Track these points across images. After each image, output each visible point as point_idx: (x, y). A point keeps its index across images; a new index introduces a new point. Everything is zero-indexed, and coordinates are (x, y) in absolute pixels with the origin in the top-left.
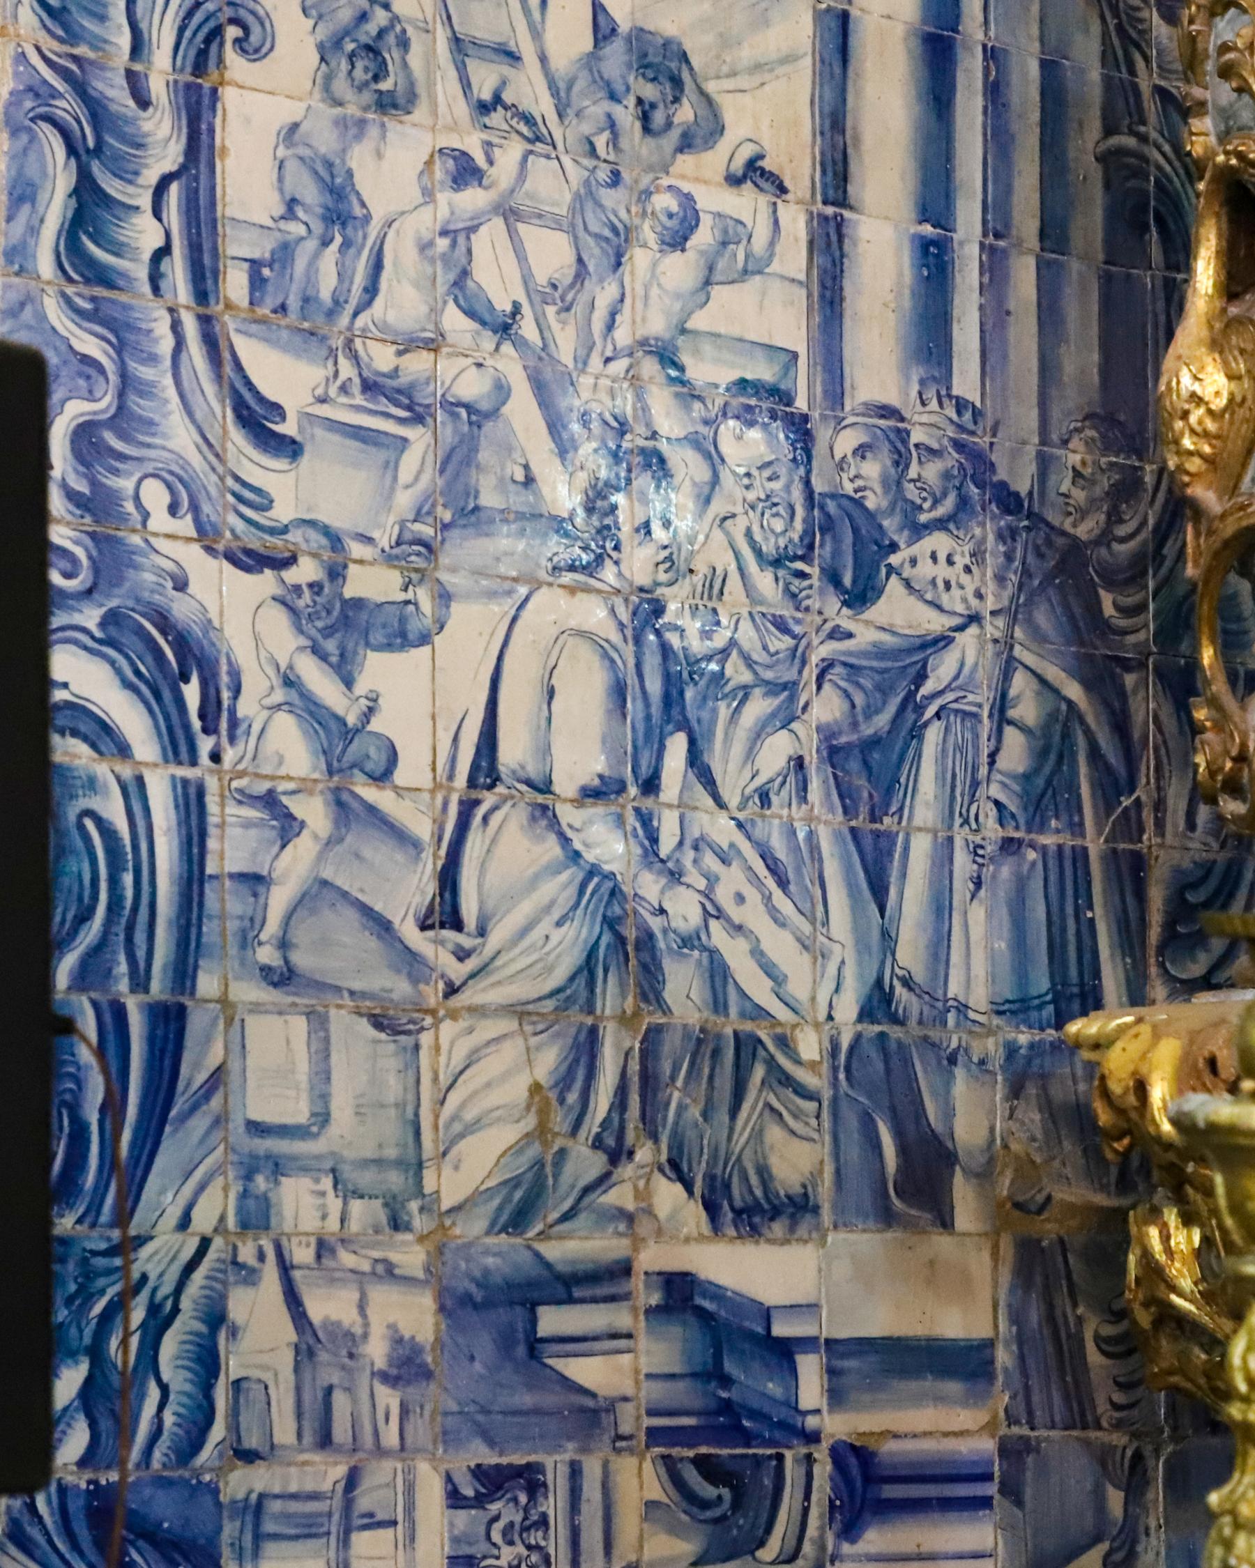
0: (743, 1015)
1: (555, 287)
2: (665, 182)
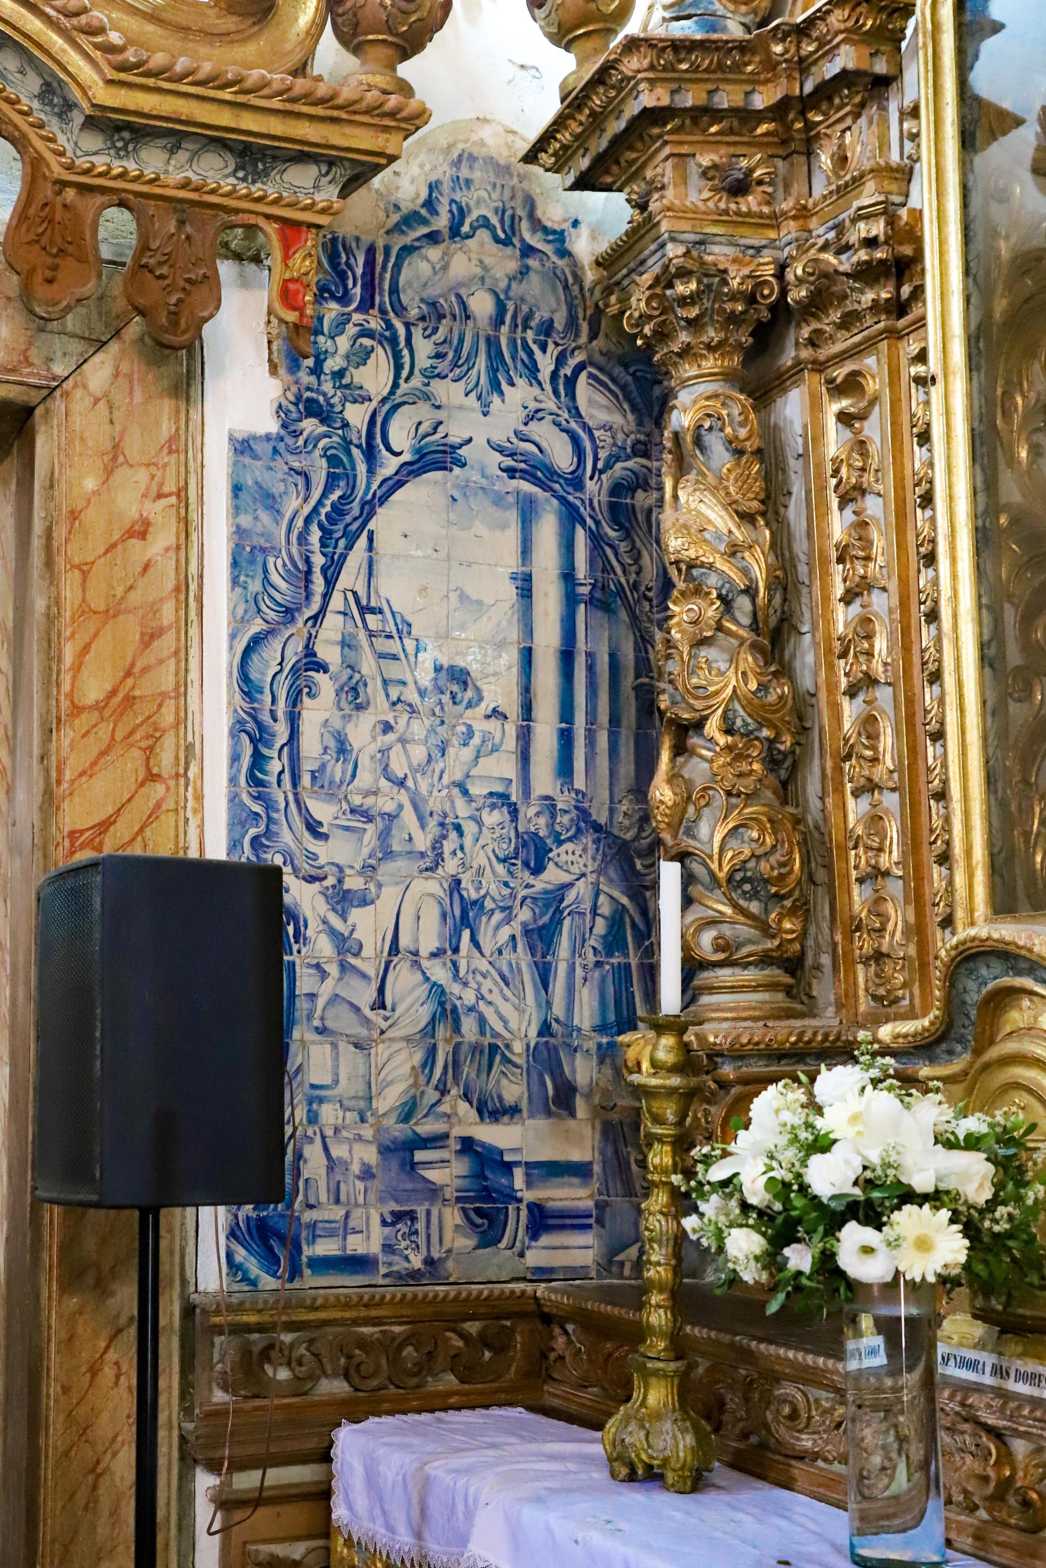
0: (492, 1036)
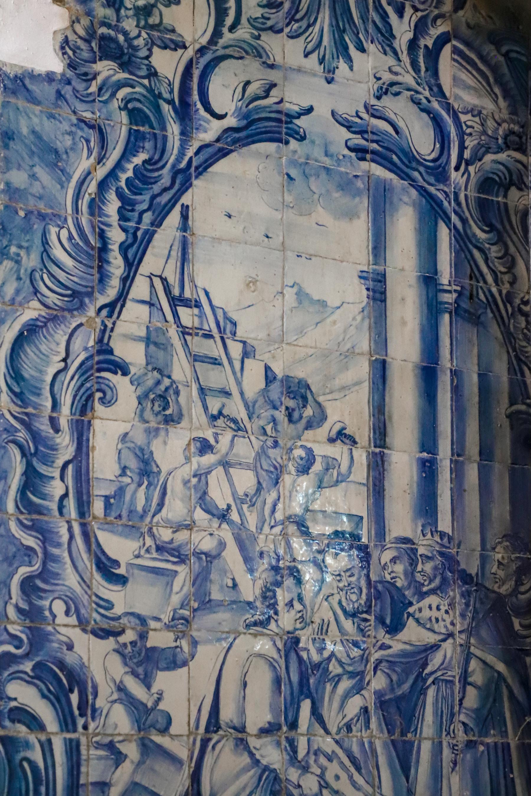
1: (247, 495)
2: (299, 443)
